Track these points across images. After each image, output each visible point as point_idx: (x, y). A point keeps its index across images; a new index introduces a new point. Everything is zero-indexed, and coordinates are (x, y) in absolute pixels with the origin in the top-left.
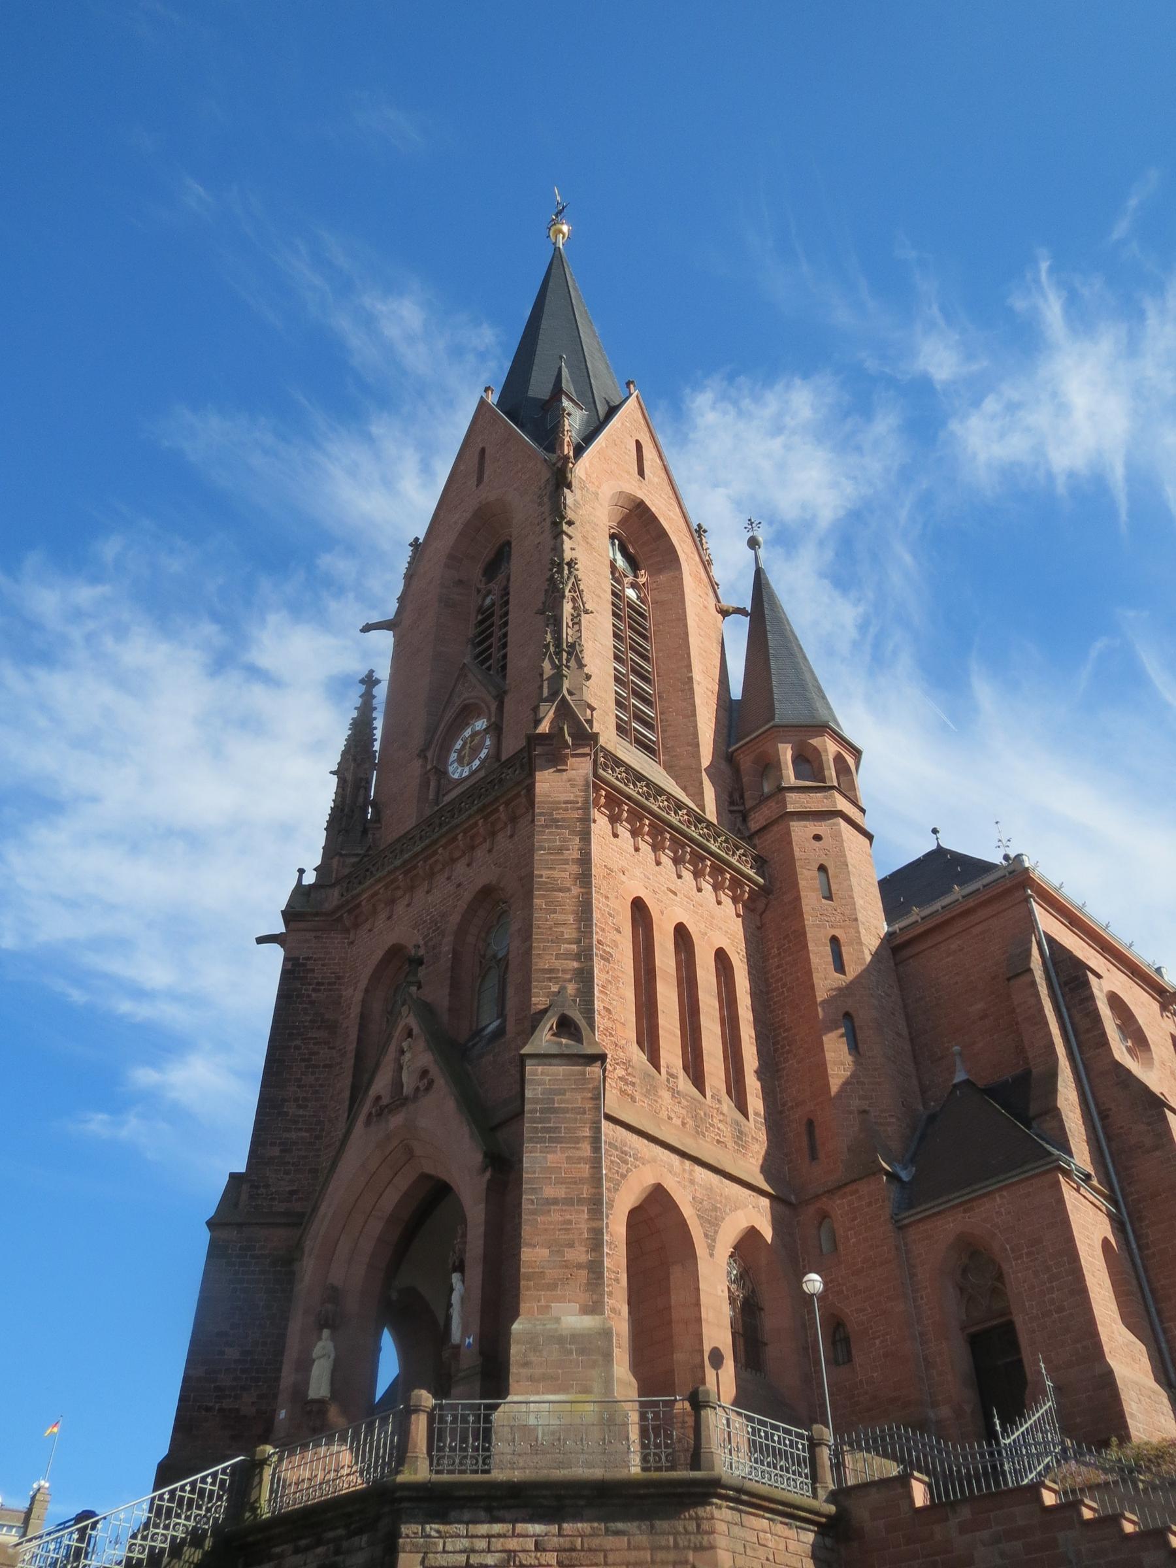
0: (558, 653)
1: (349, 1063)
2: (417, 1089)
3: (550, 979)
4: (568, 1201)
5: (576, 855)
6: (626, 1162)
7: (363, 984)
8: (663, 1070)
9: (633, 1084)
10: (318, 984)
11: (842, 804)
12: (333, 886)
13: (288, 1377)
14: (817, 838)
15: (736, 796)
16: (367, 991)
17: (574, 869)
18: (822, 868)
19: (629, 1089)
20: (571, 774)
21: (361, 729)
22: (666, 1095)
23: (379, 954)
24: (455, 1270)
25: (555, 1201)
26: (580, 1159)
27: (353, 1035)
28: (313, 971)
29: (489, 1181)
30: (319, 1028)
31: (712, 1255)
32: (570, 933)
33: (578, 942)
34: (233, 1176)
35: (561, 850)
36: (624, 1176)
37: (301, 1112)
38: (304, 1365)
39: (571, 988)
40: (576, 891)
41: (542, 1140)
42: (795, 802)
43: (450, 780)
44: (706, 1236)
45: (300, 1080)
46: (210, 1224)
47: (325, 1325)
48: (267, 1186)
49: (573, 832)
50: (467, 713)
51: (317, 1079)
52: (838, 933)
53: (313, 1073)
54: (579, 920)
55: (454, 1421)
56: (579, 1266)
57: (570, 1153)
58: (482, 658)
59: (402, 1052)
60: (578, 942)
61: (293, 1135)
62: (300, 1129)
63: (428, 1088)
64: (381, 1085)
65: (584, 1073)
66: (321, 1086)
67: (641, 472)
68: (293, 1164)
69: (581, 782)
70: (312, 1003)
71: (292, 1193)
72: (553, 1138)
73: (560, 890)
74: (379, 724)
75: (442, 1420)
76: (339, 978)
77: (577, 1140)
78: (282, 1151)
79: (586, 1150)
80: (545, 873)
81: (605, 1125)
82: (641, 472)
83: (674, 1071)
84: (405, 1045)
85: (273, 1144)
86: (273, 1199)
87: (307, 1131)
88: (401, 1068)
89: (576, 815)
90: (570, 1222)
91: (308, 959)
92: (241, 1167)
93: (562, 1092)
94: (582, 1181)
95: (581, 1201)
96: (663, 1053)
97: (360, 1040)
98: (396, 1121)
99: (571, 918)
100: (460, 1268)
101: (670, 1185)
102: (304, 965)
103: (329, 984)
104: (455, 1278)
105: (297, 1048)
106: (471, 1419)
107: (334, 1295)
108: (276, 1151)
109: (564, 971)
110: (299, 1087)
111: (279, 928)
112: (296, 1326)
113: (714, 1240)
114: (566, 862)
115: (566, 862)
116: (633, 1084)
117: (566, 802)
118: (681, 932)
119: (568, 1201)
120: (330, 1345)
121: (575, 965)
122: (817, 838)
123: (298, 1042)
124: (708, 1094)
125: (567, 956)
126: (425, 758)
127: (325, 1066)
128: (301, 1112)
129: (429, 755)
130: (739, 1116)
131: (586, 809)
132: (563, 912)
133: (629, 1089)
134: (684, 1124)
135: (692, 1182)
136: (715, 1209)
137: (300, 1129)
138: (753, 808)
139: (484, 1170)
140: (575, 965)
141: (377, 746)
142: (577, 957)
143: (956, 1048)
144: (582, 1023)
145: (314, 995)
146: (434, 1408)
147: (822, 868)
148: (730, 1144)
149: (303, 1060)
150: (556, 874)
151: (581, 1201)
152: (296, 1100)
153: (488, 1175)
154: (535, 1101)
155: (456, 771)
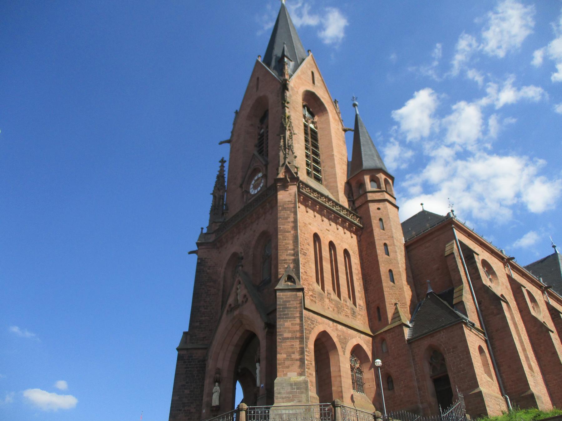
0: (285, 150)
1: (221, 293)
2: (243, 301)
3: (284, 263)
4: (292, 338)
5: (293, 220)
6: (313, 324)
7: (224, 266)
8: (326, 292)
9: (315, 297)
11: (387, 197)
12: (213, 233)
13: (205, 399)
14: (379, 209)
15: (351, 195)
16: (225, 269)
17: (292, 225)
18: (381, 220)
19: (314, 299)
20: (290, 191)
22: (327, 300)
23: (229, 256)
24: (257, 362)
25: (288, 338)
26: (296, 324)
27: (222, 283)
29: (267, 332)
31: (344, 354)
32: (291, 247)
33: (294, 250)
34: (185, 333)
35: (287, 218)
36: (312, 329)
38: (211, 394)
39: (292, 266)
40: (292, 232)
41: (283, 318)
42: (370, 196)
44: (342, 348)
46: (178, 349)
47: (217, 381)
49: (291, 212)
50: (256, 171)
52: (387, 242)
54: (294, 242)
55: (254, 413)
56: (297, 360)
57: (293, 322)
58: (261, 152)
59: (237, 289)
60: (294, 250)
63: (246, 302)
64: (231, 300)
65: (296, 295)
67: (314, 82)
69: (293, 195)
70: (207, 273)
71: (204, 338)
72: (287, 317)
73: (288, 232)
75: (250, 413)
77: (295, 318)
79: (298, 321)
80: (282, 227)
81: (305, 312)
82: (314, 82)
83: (330, 292)
84: (238, 287)
85: (197, 322)
88: (237, 295)
89: (292, 206)
90: (293, 345)
91: (206, 258)
92: (187, 330)
93: (289, 301)
94: (297, 331)
95: (296, 338)
96: (325, 286)
97: (224, 286)
98: (236, 312)
99: (291, 242)
100: (259, 361)
101: (329, 331)
104: (257, 365)
106: (252, 412)
107: (218, 371)
108: (198, 324)
109: (289, 260)
111: (195, 248)
112: (207, 381)
113: (345, 349)
115: (289, 222)
116: (315, 297)
117: (288, 201)
118: (331, 245)
119: (292, 338)
120: (218, 388)
121: (293, 258)
122: (379, 209)
124: (342, 299)
125: (290, 255)
129: (243, 186)
130: (353, 306)
131: (295, 204)
132: (288, 240)
133: (314, 299)
134: (334, 310)
135: (337, 329)
136: (345, 338)
138: (356, 199)
139: (265, 328)
140: (293, 258)
141: (226, 184)
142: (293, 255)
143: (428, 281)
144: (295, 277)
145: (208, 271)
146: (247, 409)
147: (381, 220)
148: (350, 316)
150: (285, 227)
151: (296, 338)
153: (266, 330)
154: (280, 305)
155: (253, 192)
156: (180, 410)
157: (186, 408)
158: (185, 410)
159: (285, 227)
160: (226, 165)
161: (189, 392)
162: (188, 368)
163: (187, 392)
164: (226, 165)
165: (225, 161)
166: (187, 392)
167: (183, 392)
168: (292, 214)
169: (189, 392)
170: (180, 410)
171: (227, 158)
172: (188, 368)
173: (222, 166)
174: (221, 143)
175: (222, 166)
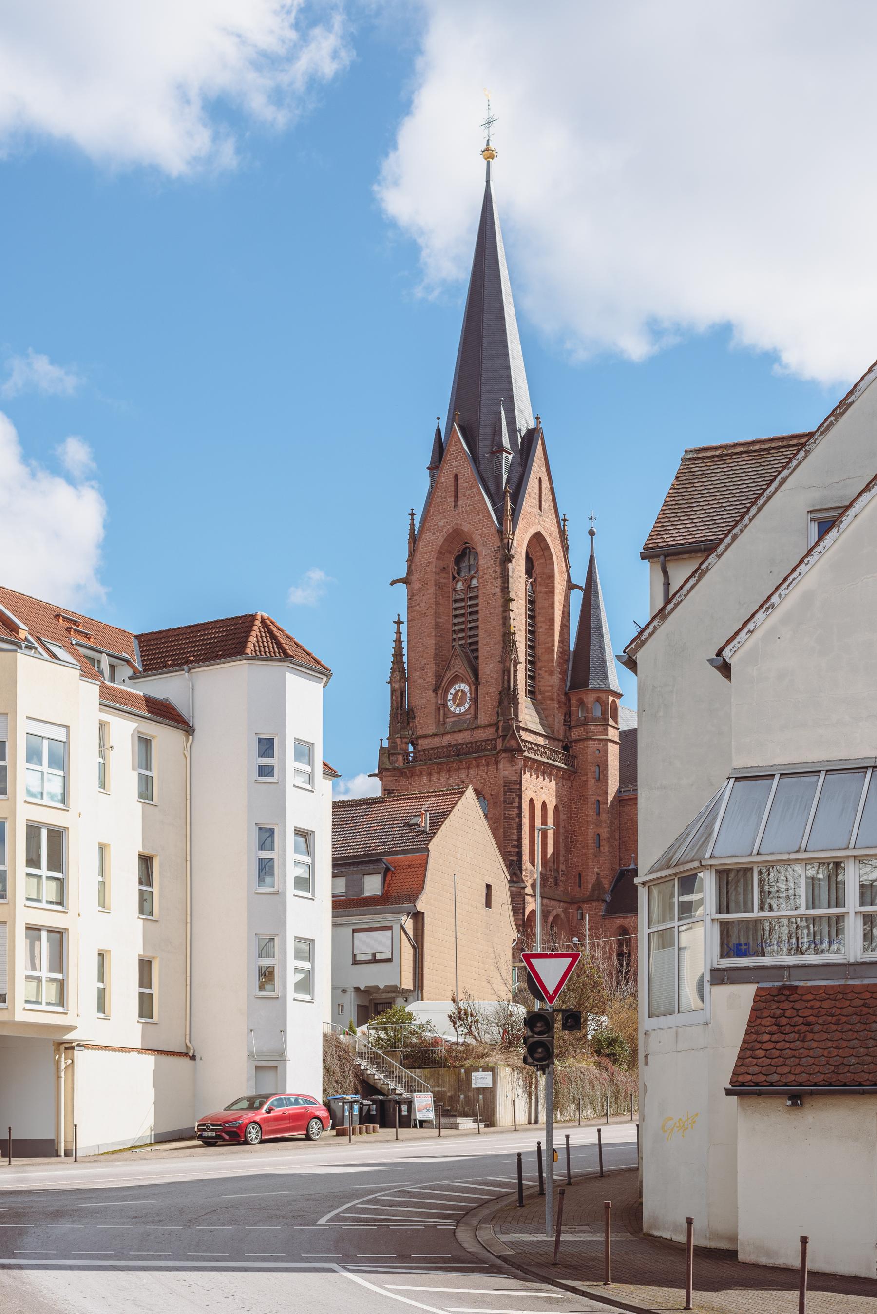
17: (516, 811)
21: (398, 654)
32: (515, 837)
33: (518, 841)
39: (515, 859)
40: (517, 820)
43: (449, 710)
50: (456, 679)
60: (518, 841)
74: (405, 645)
99: (515, 832)
114: (514, 808)
115: (514, 808)
126: (437, 694)
141: (406, 665)
150: (510, 813)
159: (510, 813)
160: (404, 628)
164: (404, 628)
165: (403, 623)
168: (517, 799)
171: (404, 618)
173: (399, 632)
174: (393, 583)
175: (399, 632)
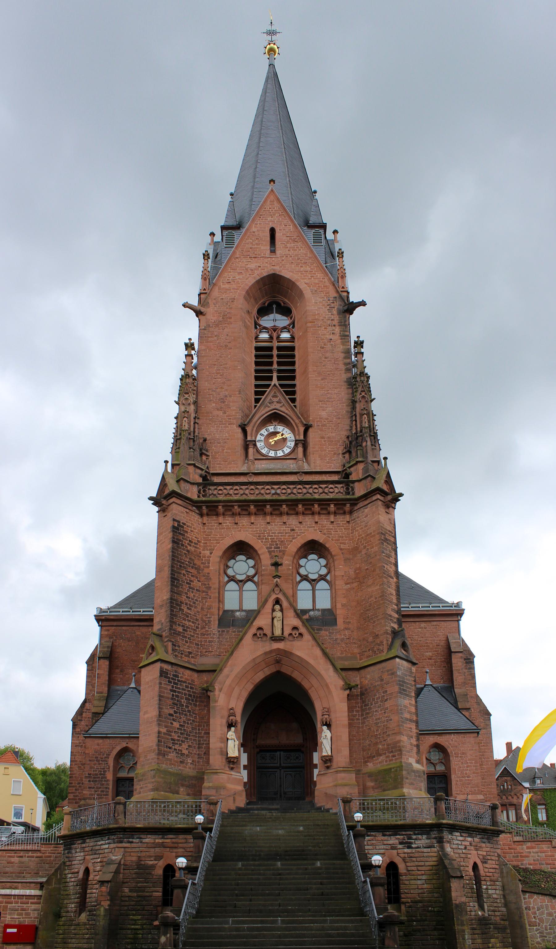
10: (190, 541)
28: (187, 532)
30: (192, 567)
37: (189, 611)
45: (187, 594)
48: (179, 646)
51: (194, 596)
53: (192, 592)
61: (187, 623)
62: (190, 621)
66: (196, 600)
68: (189, 638)
70: (188, 551)
76: (198, 541)
78: (183, 630)
85: (179, 625)
86: (182, 654)
87: (193, 622)
91: (184, 524)
102: (183, 527)
103: (195, 544)
105: (184, 575)
108: (180, 629)
110: (187, 597)
112: (217, 723)
123: (184, 572)
127: (197, 590)
128: (189, 611)
137: (190, 621)
149: (187, 583)
152: (186, 604)
156: (170, 748)
157: (177, 747)
158: (175, 749)
161: (178, 726)
162: (175, 691)
163: (176, 725)
166: (176, 725)
167: (172, 723)
169: (178, 726)
170: (170, 748)
172: (175, 691)
